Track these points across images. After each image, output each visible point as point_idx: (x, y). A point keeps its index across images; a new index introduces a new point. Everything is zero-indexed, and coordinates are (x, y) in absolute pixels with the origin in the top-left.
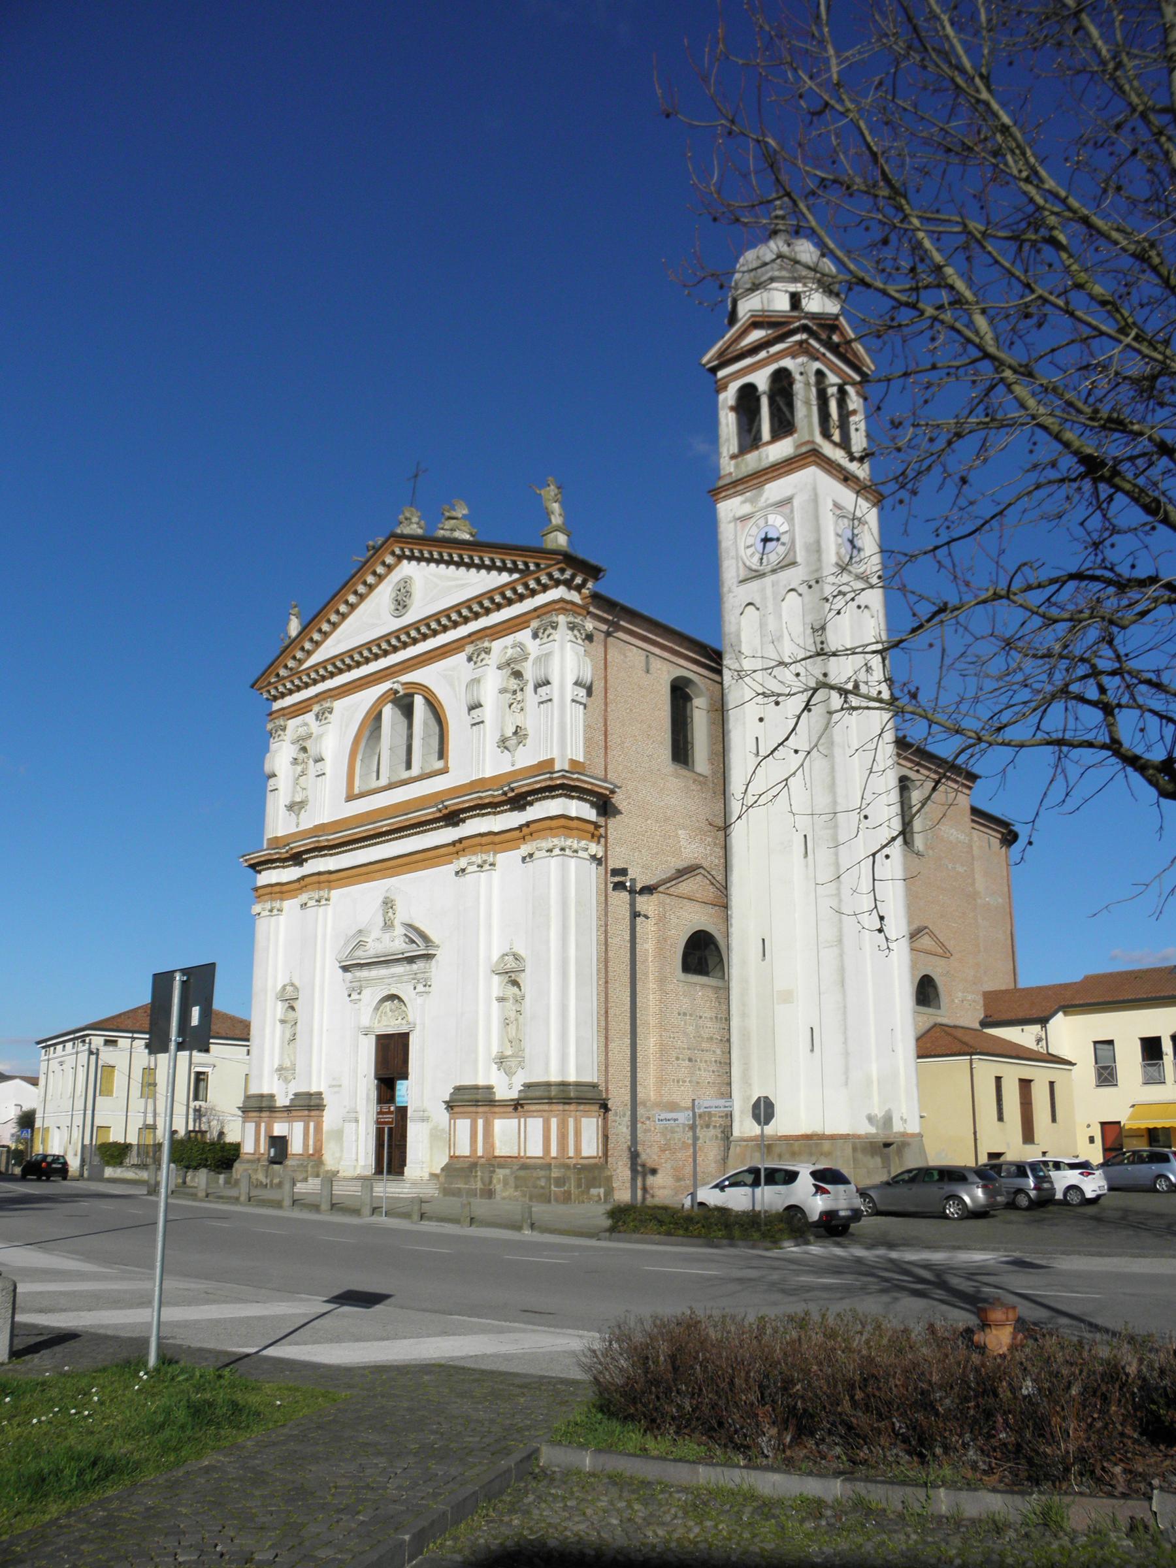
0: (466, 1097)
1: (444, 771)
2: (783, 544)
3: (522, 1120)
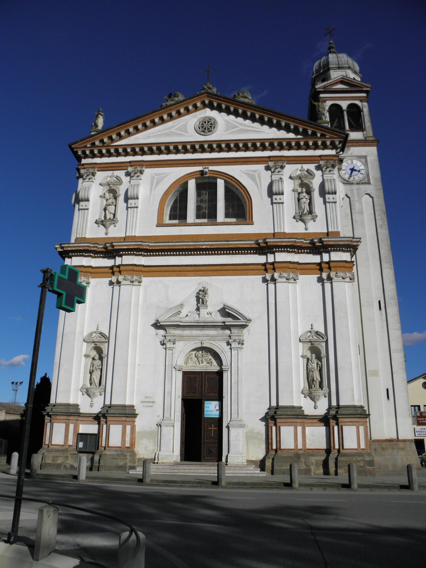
0: (289, 413)
2: (362, 174)
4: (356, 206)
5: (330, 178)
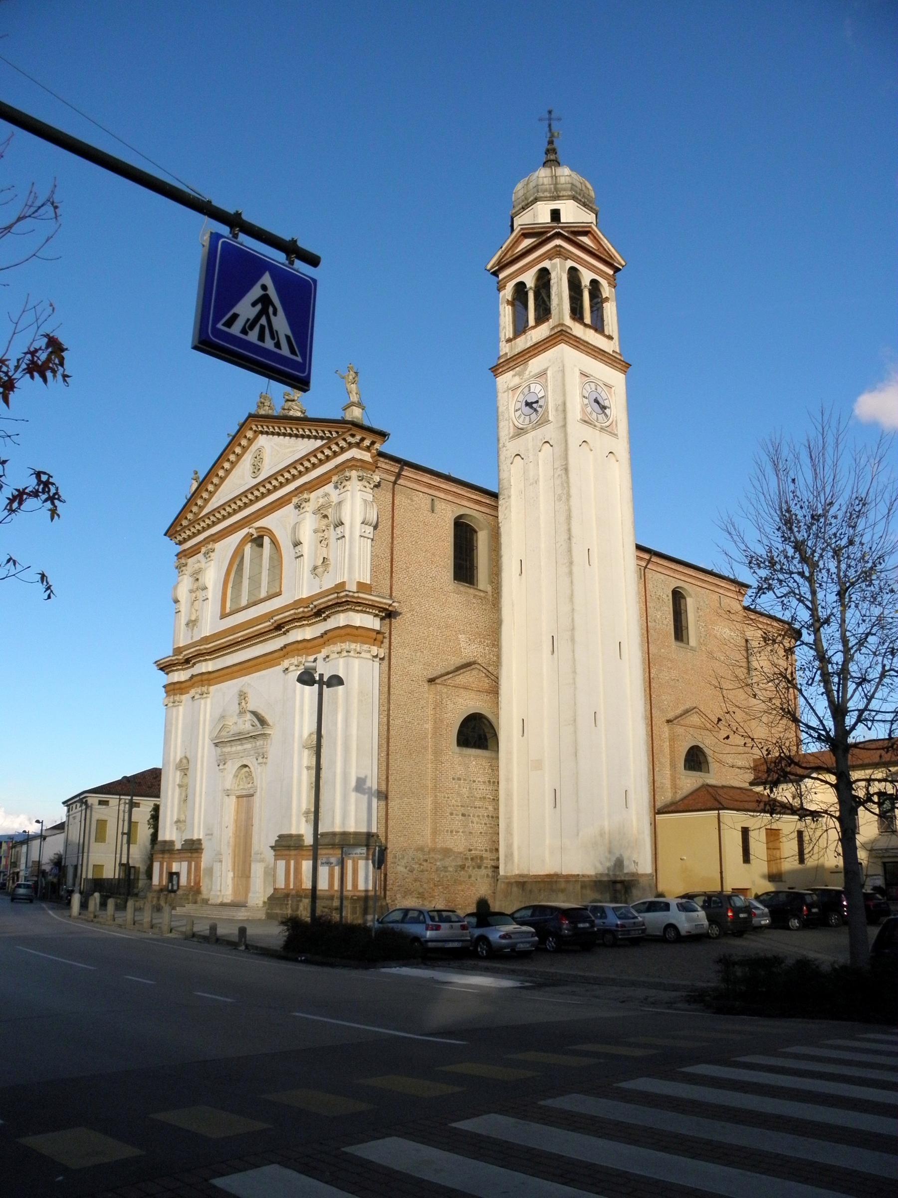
1: (279, 594)
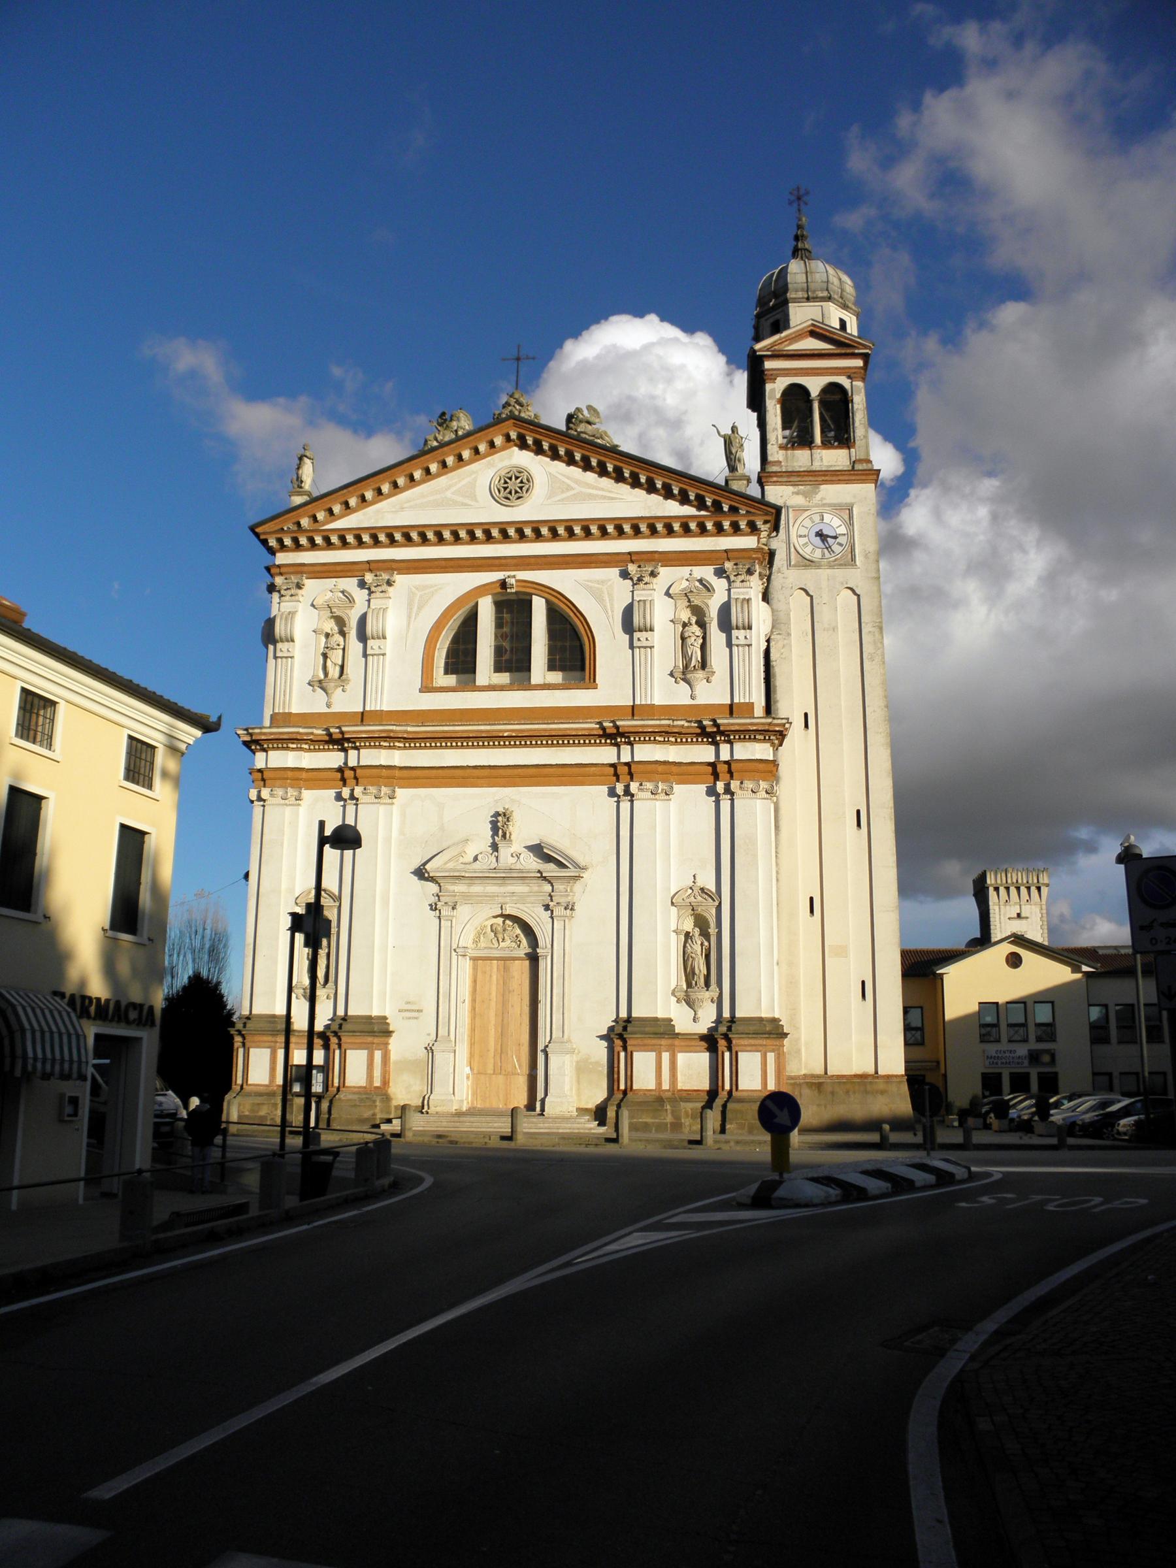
3: (666, 1056)
4: (824, 615)
5: (742, 597)
